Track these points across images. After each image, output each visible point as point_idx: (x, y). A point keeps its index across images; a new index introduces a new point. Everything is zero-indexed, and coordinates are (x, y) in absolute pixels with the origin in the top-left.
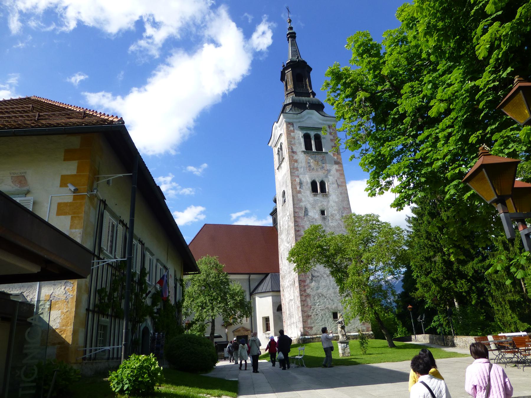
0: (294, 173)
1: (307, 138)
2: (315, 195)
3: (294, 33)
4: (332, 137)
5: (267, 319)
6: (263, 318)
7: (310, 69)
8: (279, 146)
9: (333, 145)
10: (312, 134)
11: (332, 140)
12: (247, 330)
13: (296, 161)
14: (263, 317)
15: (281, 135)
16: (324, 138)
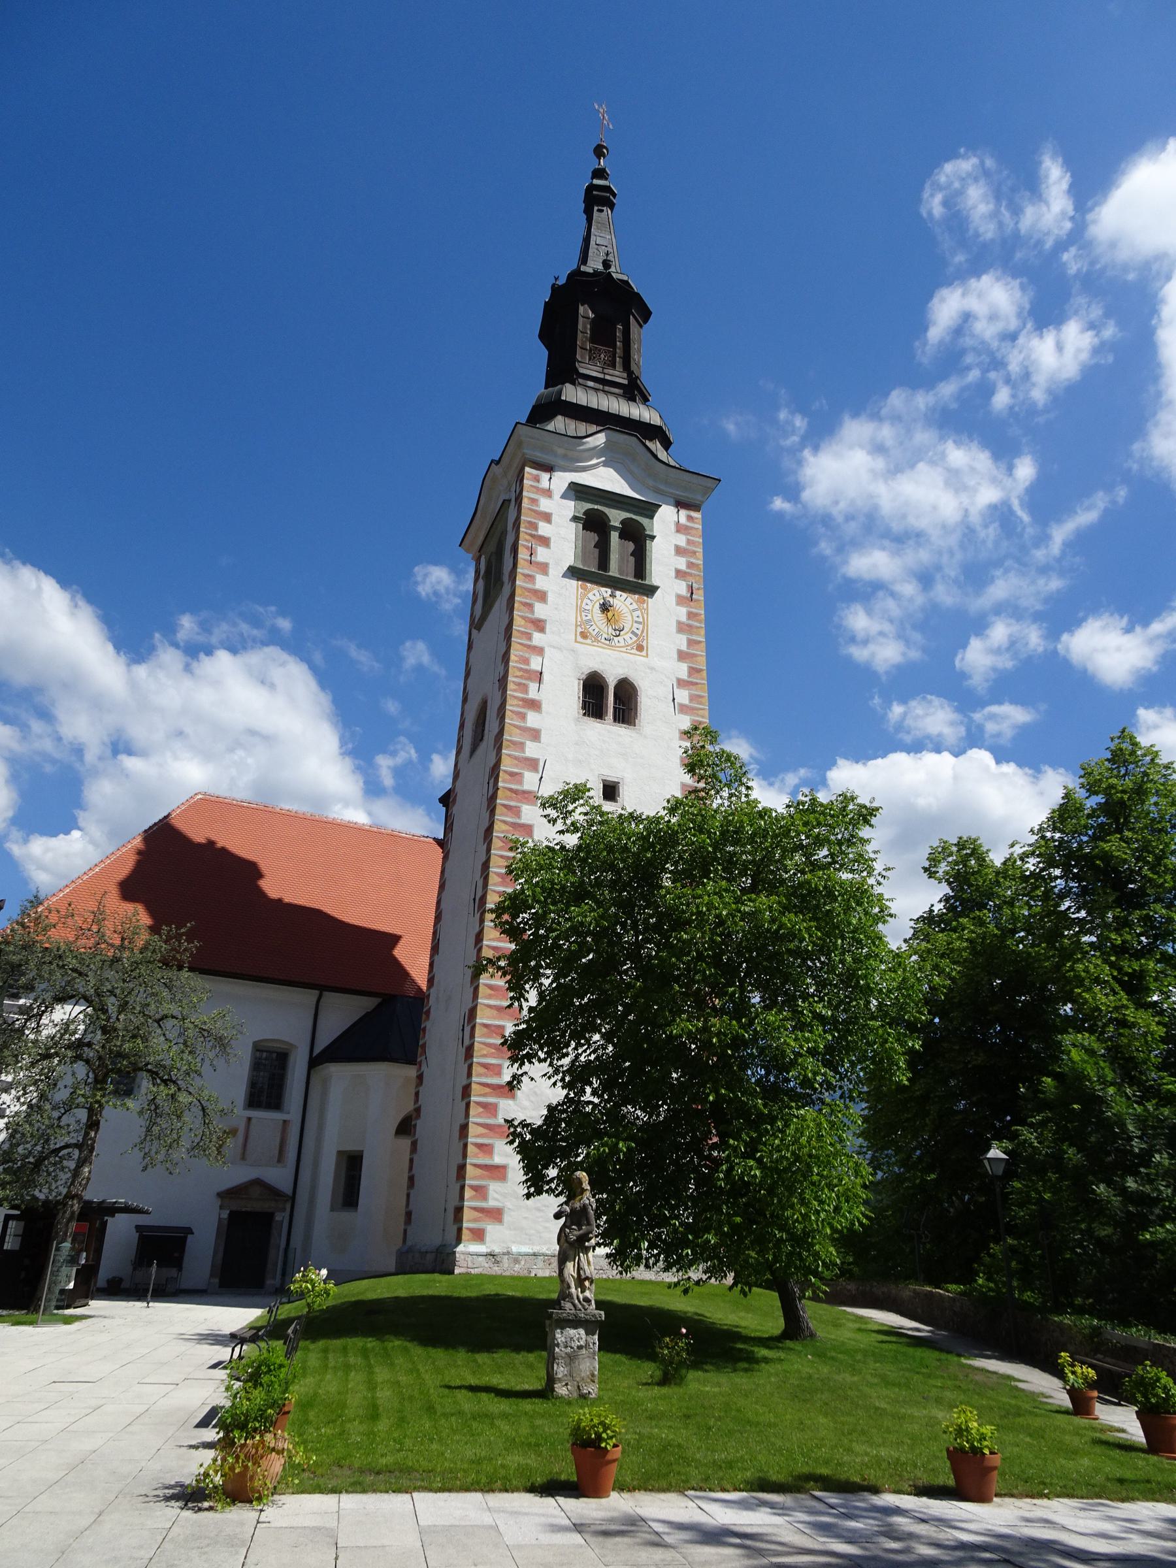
0: (529, 637)
1: (593, 523)
2: (593, 724)
3: (608, 189)
4: (681, 540)
5: (352, 1164)
6: (340, 1153)
7: (646, 314)
8: (492, 547)
9: (683, 567)
10: (616, 517)
11: (679, 551)
12: (272, 1192)
13: (542, 596)
14: (340, 1153)
15: (506, 503)
16: (653, 538)
